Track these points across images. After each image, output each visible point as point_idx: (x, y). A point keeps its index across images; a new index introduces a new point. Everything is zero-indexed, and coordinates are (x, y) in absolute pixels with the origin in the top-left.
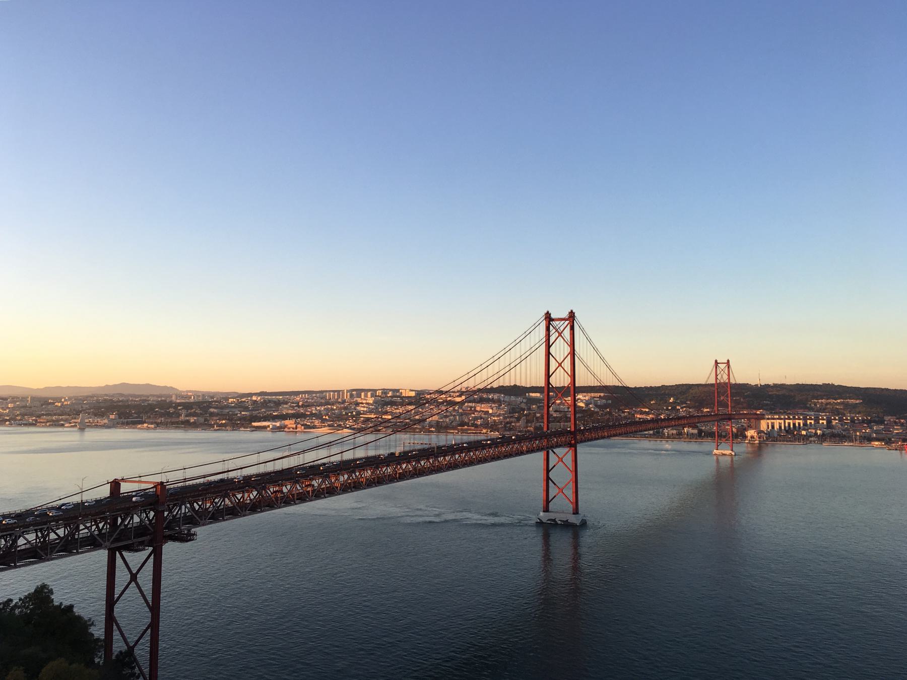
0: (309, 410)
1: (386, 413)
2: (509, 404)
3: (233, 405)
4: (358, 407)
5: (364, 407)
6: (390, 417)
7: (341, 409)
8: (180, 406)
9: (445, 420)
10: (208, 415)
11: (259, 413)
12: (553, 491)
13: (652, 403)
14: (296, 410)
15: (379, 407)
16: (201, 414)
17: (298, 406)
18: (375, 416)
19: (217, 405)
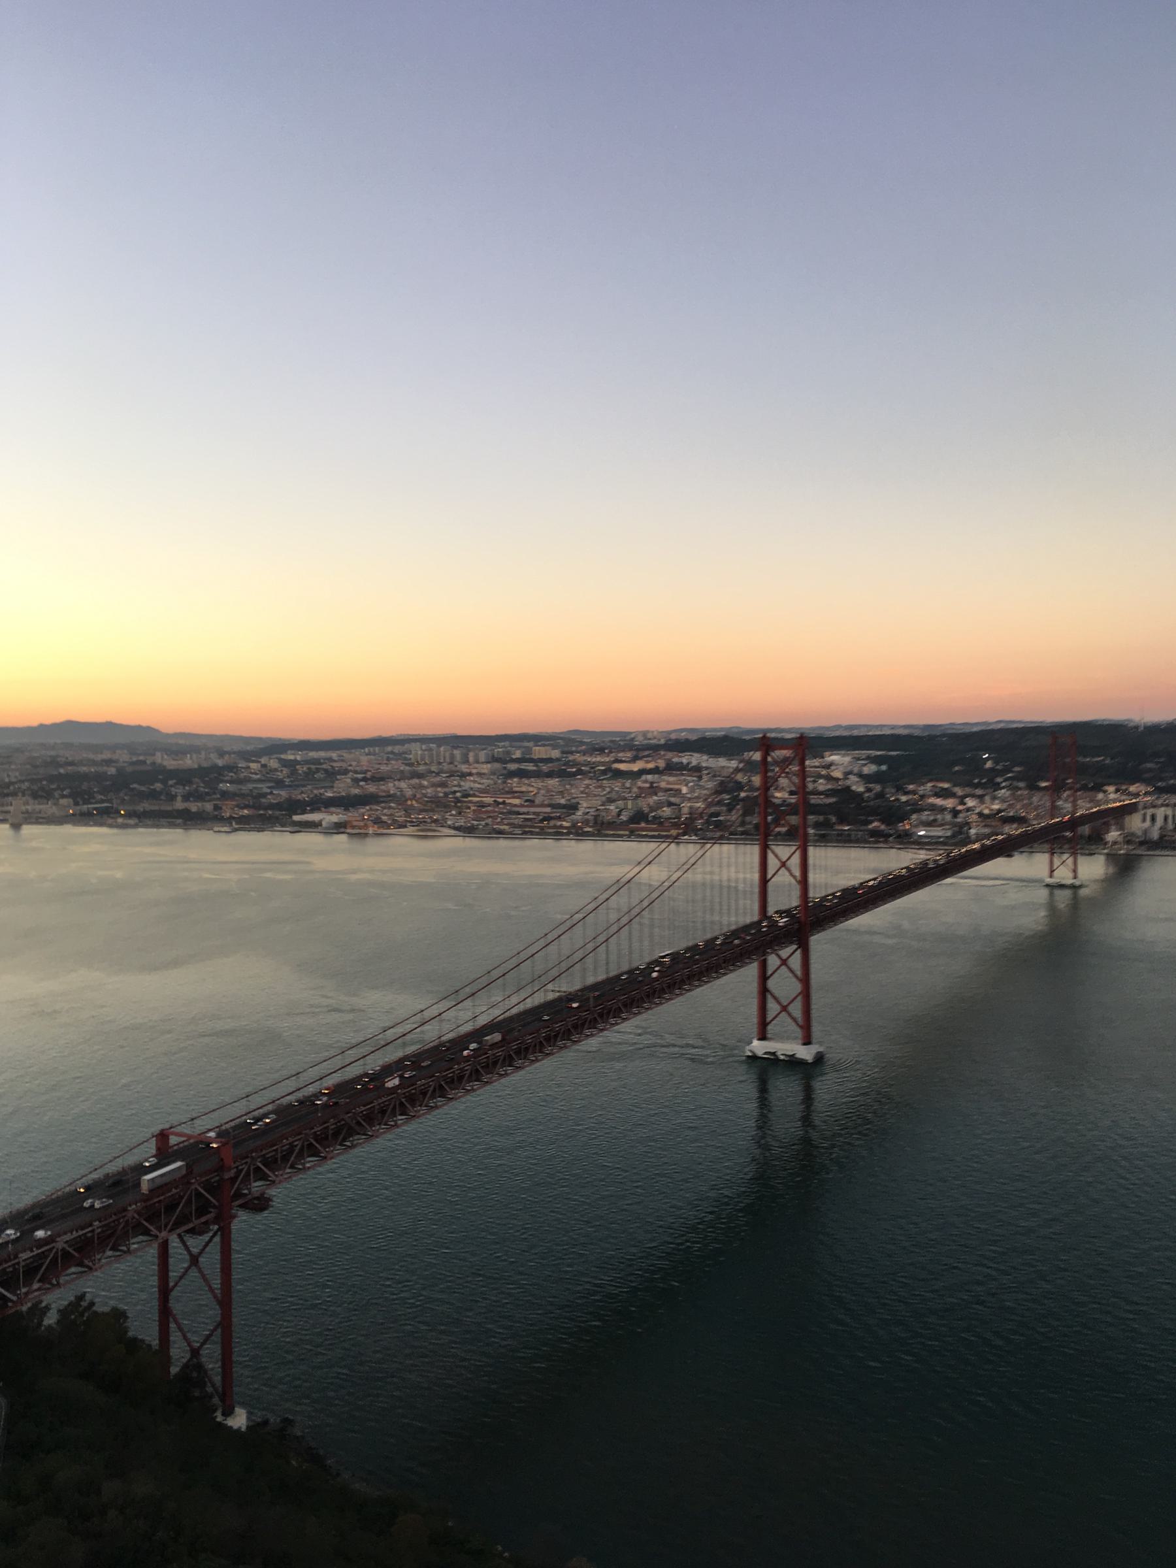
0: (383, 787)
1: (512, 792)
2: (714, 774)
3: (258, 776)
4: (464, 781)
5: (475, 782)
6: (517, 801)
7: (434, 785)
8: (172, 779)
9: (608, 807)
10: (218, 796)
11: (302, 793)
12: (773, 1007)
13: (956, 768)
14: (362, 787)
15: (500, 781)
16: (207, 794)
17: (364, 779)
18: (493, 799)
19: (232, 776)
